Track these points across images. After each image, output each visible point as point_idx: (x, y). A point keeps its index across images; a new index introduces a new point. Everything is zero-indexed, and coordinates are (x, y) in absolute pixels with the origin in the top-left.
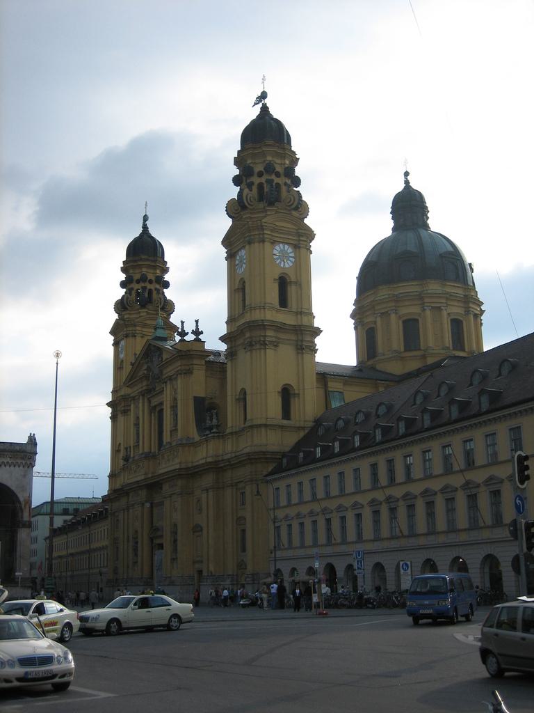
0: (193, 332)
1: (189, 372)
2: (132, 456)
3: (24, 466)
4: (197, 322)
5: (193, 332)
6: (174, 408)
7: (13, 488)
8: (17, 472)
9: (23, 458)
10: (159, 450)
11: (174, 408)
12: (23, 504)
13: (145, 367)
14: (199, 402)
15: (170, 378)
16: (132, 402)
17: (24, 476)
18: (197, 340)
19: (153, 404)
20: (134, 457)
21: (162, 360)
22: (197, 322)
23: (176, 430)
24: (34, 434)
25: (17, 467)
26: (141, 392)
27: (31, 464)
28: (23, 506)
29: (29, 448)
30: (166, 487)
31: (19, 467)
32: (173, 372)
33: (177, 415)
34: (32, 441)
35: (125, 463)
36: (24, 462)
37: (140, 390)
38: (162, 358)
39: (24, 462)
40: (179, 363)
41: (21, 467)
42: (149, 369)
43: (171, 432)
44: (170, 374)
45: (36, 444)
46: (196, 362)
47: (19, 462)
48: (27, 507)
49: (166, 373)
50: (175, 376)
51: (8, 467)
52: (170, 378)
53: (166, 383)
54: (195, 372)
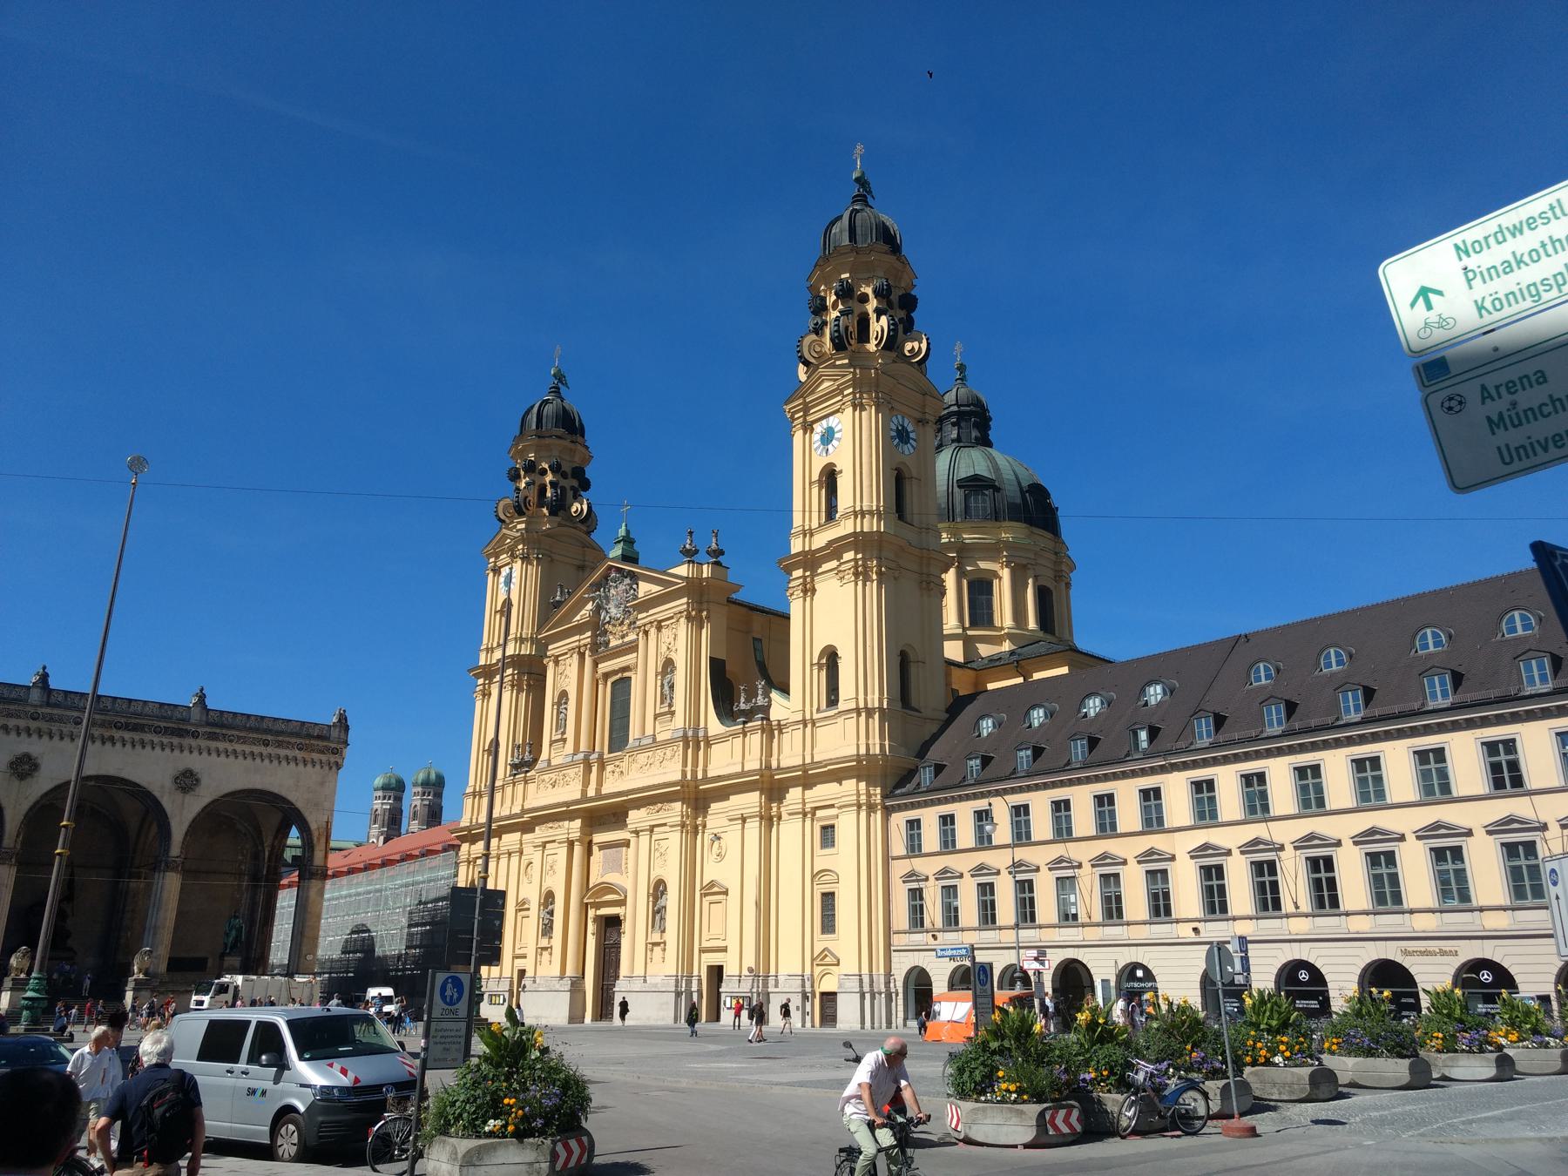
7: (299, 805)
8: (311, 774)
9: (322, 752)
12: (315, 834)
13: (590, 606)
17: (322, 784)
19: (604, 667)
21: (636, 597)
26: (579, 647)
27: (337, 763)
28: (315, 839)
30: (636, 817)
37: (577, 643)
44: (660, 617)
45: (347, 728)
47: (316, 756)
48: (323, 840)
53: (646, 633)
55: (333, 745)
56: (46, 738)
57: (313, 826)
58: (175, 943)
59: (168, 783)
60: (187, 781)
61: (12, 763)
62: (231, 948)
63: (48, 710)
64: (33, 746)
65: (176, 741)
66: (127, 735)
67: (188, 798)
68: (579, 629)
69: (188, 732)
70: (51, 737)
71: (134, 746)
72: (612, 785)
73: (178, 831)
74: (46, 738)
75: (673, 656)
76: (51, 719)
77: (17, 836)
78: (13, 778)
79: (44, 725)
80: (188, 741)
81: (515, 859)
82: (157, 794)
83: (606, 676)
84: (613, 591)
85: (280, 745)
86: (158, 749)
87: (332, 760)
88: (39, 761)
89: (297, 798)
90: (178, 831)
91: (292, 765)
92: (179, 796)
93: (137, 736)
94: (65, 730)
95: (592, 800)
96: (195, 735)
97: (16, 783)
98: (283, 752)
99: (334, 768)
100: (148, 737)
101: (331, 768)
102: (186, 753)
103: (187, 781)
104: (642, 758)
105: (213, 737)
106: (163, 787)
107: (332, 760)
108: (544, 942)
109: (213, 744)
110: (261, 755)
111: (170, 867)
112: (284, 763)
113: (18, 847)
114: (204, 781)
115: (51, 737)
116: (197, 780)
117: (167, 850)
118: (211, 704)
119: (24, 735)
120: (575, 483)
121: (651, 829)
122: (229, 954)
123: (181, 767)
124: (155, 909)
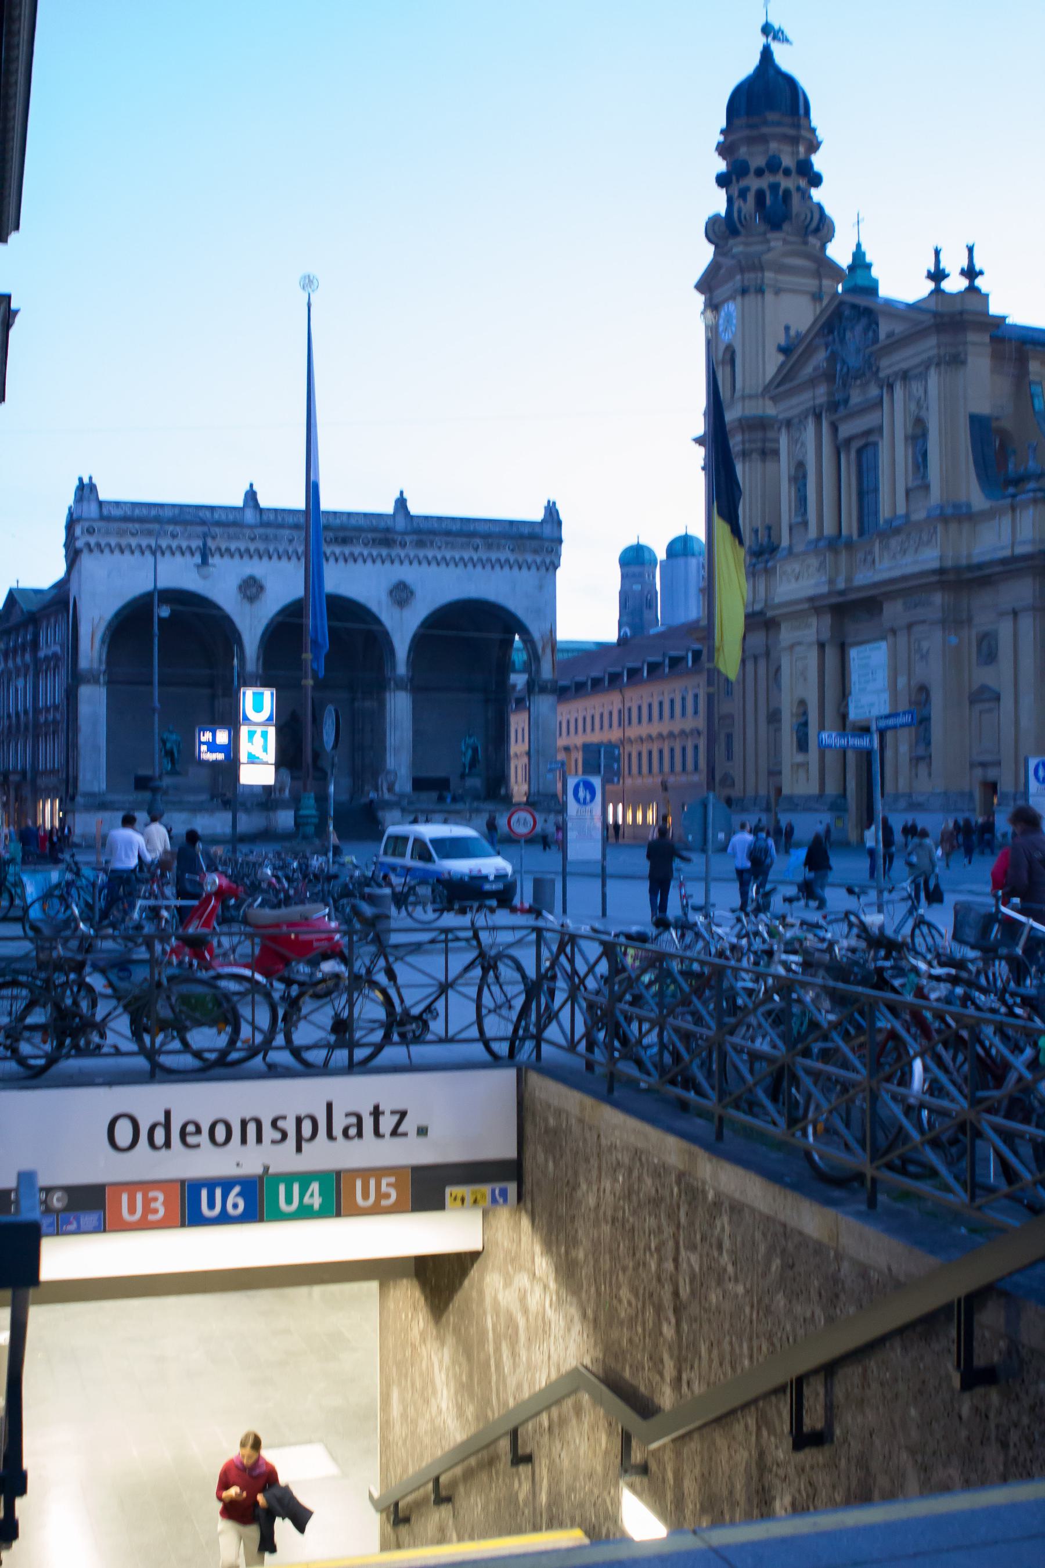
0: (963, 273)
1: (956, 361)
2: (785, 542)
3: (538, 569)
4: (971, 250)
5: (963, 273)
6: (918, 436)
8: (527, 578)
9: (536, 552)
10: (861, 532)
11: (918, 436)
14: (979, 425)
15: (905, 376)
16: (784, 430)
17: (541, 587)
18: (972, 289)
20: (790, 547)
21: (876, 340)
22: (971, 250)
23: (926, 487)
24: (554, 503)
25: (524, 569)
28: (540, 651)
29: (547, 530)
31: (529, 568)
32: (917, 360)
33: (925, 455)
34: (552, 512)
35: (754, 560)
36: (539, 560)
38: (876, 333)
39: (539, 560)
40: (932, 341)
41: (534, 568)
42: (833, 358)
43: (908, 492)
44: (904, 365)
46: (972, 337)
47: (530, 558)
48: (549, 651)
49: (890, 366)
50: (921, 369)
51: (506, 568)
52: (905, 376)
53: (891, 387)
54: (970, 359)
55: (546, 544)
56: (265, 559)
57: (536, 635)
58: (416, 761)
59: (384, 597)
60: (401, 594)
61: (240, 587)
62: (470, 768)
63: (262, 531)
64: (257, 568)
65: (384, 552)
66: (338, 550)
67: (407, 613)
68: (812, 382)
69: (394, 542)
70: (270, 558)
71: (346, 560)
72: (864, 577)
73: (401, 647)
74: (265, 559)
75: (923, 414)
76: (266, 538)
77: (258, 659)
78: (245, 601)
79: (262, 546)
80: (397, 551)
81: (762, 664)
82: (374, 608)
83: (848, 441)
84: (848, 335)
85: (489, 547)
86: (369, 562)
87: (548, 561)
88: (264, 582)
89: (516, 605)
90: (401, 647)
91: (506, 568)
92: (396, 611)
93: (347, 550)
94: (281, 550)
95: (841, 593)
96: (403, 545)
97: (247, 605)
98: (494, 556)
99: (551, 568)
100: (357, 550)
101: (547, 569)
102: (397, 563)
103: (401, 594)
104: (894, 543)
105: (420, 544)
106: (379, 603)
107: (548, 561)
108: (800, 758)
109: (421, 553)
110: (471, 559)
111: (400, 686)
112: (497, 568)
113: (260, 671)
114: (419, 593)
115: (270, 558)
116: (412, 593)
117: (394, 667)
118: (416, 508)
119: (246, 558)
120: (803, 183)
121: (910, 626)
122: (470, 774)
123: (394, 580)
124: (393, 727)
